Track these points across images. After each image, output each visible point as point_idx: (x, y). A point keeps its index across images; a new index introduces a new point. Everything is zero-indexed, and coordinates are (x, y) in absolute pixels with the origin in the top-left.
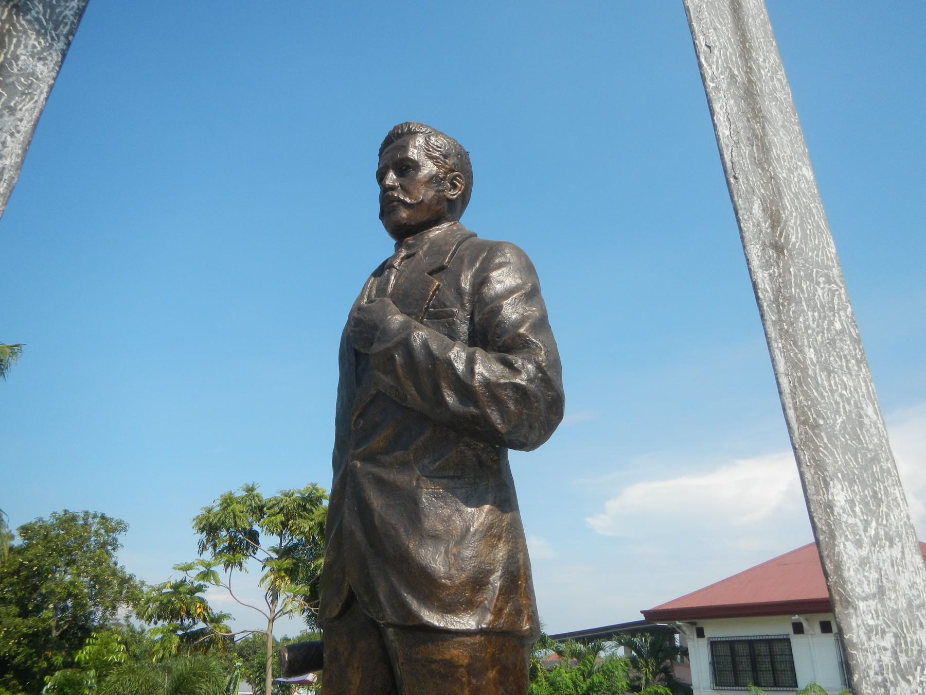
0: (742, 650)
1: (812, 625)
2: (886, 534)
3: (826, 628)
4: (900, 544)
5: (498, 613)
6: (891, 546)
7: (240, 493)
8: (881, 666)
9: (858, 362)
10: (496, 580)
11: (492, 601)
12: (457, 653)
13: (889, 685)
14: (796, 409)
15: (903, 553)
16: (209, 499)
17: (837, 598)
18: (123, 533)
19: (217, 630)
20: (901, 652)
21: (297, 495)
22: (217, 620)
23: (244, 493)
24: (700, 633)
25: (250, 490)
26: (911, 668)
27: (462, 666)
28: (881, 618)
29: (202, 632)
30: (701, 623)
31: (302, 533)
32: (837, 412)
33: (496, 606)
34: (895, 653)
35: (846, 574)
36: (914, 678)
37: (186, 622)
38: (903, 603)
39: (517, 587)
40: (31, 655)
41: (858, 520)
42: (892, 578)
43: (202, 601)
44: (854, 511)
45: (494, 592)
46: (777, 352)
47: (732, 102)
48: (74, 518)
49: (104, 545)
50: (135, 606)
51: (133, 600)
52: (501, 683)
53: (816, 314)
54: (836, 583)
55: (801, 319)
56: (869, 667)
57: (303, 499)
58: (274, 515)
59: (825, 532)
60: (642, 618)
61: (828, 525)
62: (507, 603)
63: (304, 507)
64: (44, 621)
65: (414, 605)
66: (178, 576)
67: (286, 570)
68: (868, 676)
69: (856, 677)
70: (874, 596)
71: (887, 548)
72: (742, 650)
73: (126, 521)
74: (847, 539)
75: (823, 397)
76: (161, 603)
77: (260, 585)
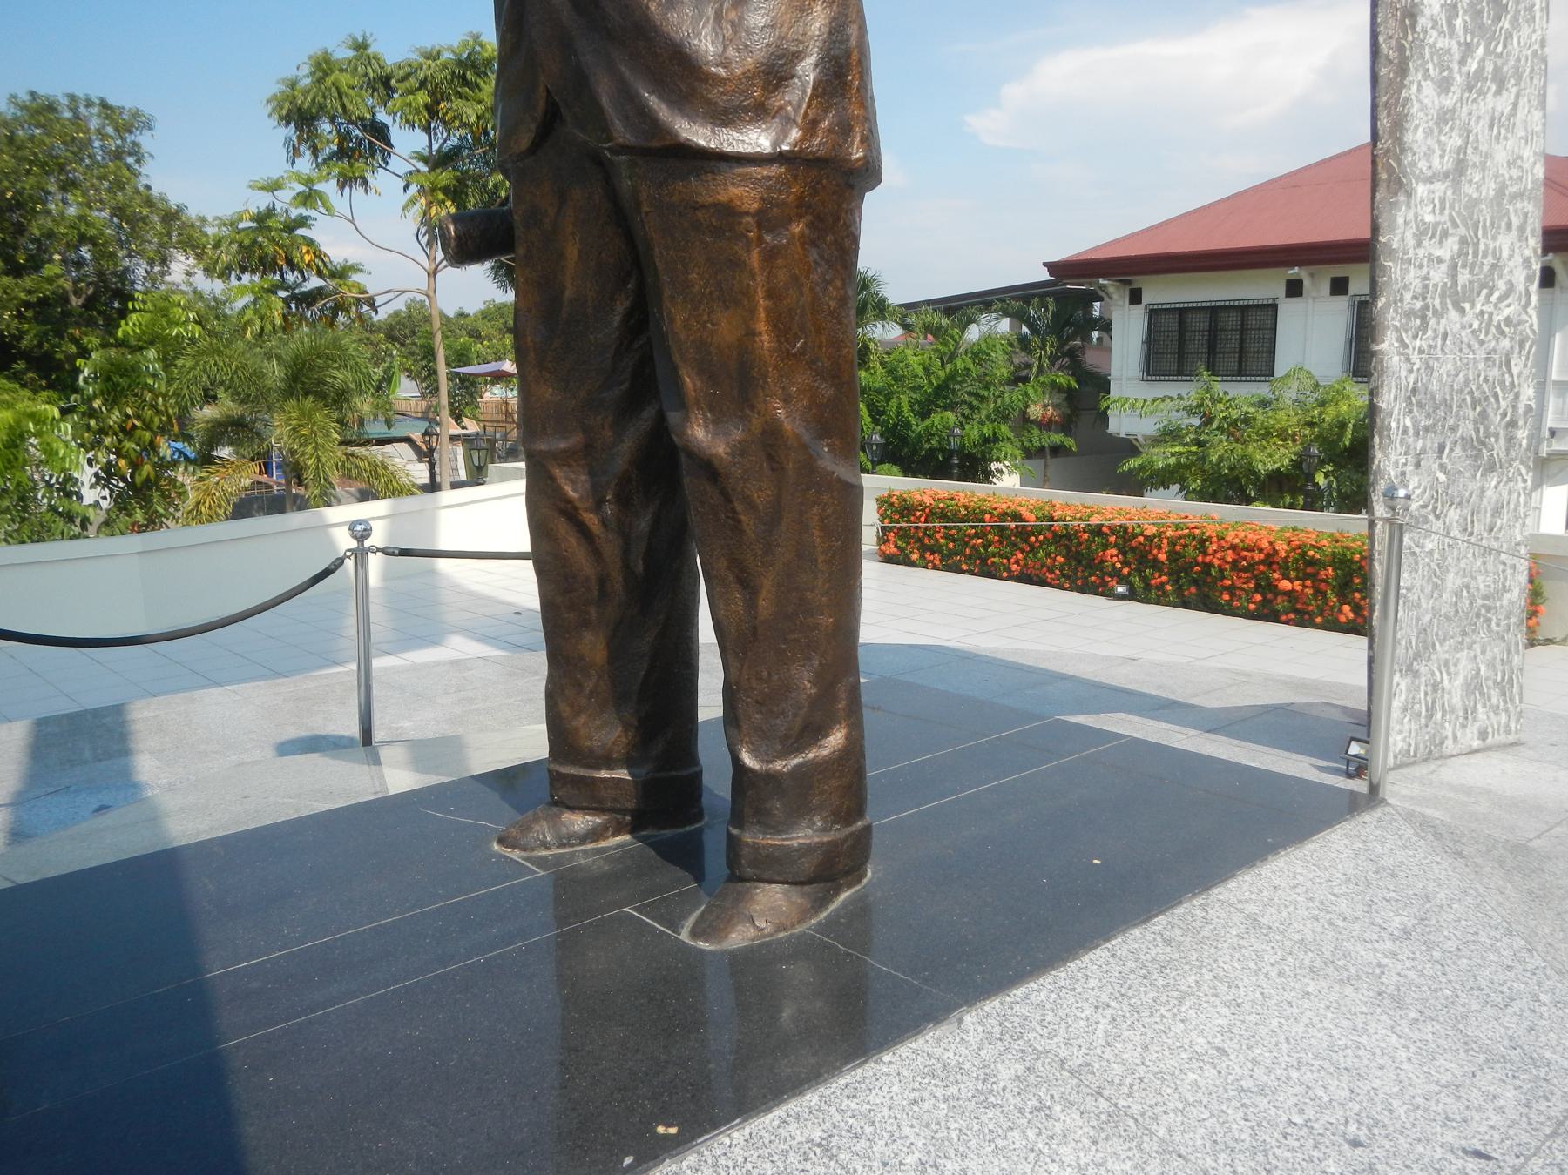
0: (1198, 323)
1: (1317, 283)
2: (1497, 70)
3: (1339, 287)
4: (1514, 90)
5: (810, 127)
6: (1498, 92)
7: (344, 53)
8: (1426, 287)
10: (807, 70)
11: (799, 106)
12: (741, 193)
13: (1430, 314)
15: (1515, 105)
16: (291, 64)
17: (1384, 176)
18: (147, 133)
19: (344, 290)
20: (1464, 266)
21: (447, 56)
22: (341, 273)
23: (351, 54)
24: (1136, 297)
25: (361, 46)
26: (1472, 291)
27: (747, 213)
28: (1447, 212)
29: (319, 293)
30: (1140, 281)
31: (464, 125)
33: (806, 114)
34: (1454, 268)
35: (1408, 137)
36: (1473, 306)
37: (291, 277)
38: (1490, 189)
39: (845, 86)
40: (45, 334)
41: (1454, 43)
42: (1484, 148)
43: (310, 242)
44: (1451, 26)
45: (804, 92)
48: (51, 108)
49: (118, 155)
50: (199, 257)
51: (193, 248)
52: (814, 244)
54: (1388, 151)
56: (1406, 287)
57: (459, 63)
58: (411, 92)
59: (1391, 62)
60: (1044, 275)
61: (1401, 49)
62: (826, 111)
63: (464, 77)
64: (50, 280)
65: (663, 112)
66: (261, 201)
67: (445, 190)
68: (1401, 300)
69: (1381, 302)
70: (1446, 176)
71: (1490, 96)
72: (1198, 323)
73: (147, 109)
74: (1426, 76)
76: (240, 244)
77: (403, 216)
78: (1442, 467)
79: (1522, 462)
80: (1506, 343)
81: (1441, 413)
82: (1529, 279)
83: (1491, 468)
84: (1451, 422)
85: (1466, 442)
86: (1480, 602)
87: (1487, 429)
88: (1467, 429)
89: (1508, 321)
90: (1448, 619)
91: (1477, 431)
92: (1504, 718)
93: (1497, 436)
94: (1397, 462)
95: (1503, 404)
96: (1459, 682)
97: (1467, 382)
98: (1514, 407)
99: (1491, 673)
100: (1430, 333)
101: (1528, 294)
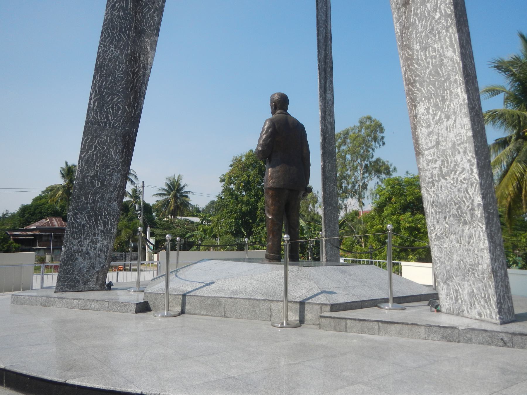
4: (454, 118)
6: (448, 120)
8: (432, 176)
13: (435, 182)
20: (444, 167)
26: (448, 173)
34: (441, 169)
35: (420, 142)
36: (450, 177)
38: (450, 145)
41: (430, 116)
42: (445, 136)
53: (423, 22)
55: (414, 32)
70: (434, 147)
74: (422, 126)
75: (420, 65)
78: (447, 223)
79: (479, 222)
80: (465, 185)
81: (444, 208)
82: (472, 165)
83: (465, 223)
84: (448, 210)
85: (454, 216)
86: (469, 266)
87: (461, 211)
88: (454, 211)
89: (464, 179)
90: (457, 269)
91: (458, 212)
92: (488, 312)
93: (466, 214)
94: (431, 222)
95: (467, 204)
96: (466, 292)
97: (452, 198)
98: (472, 204)
99: (478, 292)
100: (436, 187)
101: (472, 170)
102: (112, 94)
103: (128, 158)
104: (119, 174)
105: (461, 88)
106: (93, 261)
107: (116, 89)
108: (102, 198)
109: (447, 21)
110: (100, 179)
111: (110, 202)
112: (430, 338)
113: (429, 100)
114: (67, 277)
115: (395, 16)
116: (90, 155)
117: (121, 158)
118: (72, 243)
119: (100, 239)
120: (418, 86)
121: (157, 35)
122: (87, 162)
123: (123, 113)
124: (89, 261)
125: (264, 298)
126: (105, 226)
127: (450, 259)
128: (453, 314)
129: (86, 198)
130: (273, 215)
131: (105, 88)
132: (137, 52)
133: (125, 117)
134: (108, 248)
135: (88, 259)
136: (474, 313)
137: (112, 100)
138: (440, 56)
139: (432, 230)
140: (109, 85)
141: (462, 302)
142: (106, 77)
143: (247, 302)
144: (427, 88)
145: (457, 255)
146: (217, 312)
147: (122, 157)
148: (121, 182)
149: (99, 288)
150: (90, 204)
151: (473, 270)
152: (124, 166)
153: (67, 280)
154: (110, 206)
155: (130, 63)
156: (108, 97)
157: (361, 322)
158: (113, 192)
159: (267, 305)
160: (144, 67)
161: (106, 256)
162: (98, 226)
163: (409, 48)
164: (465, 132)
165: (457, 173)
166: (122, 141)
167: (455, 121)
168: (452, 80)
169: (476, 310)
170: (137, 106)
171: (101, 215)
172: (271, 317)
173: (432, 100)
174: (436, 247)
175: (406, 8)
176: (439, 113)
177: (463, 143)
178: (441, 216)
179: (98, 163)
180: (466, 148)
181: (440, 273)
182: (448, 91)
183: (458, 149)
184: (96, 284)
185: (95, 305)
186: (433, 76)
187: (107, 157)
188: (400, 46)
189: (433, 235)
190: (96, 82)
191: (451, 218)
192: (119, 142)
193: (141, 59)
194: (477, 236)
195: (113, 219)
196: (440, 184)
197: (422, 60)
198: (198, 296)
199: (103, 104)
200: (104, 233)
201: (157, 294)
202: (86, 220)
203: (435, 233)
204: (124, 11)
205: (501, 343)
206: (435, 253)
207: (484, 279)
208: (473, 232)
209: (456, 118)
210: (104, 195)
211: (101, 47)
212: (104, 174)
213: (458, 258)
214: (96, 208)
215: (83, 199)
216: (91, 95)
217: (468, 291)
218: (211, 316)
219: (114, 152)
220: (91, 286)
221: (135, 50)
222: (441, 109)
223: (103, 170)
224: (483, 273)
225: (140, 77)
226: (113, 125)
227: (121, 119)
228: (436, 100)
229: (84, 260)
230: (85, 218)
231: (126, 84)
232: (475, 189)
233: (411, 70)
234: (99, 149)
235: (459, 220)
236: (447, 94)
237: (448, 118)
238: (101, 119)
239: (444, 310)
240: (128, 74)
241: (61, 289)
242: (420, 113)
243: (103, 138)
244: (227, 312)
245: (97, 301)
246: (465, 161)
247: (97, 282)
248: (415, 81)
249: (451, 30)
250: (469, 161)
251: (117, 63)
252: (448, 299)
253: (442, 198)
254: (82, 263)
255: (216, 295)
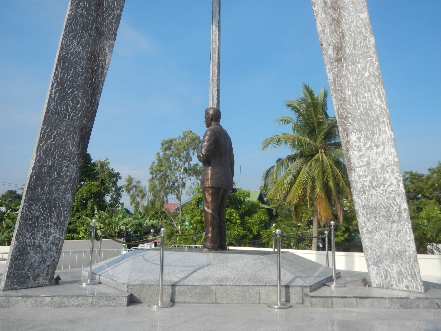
4: (382, 147)
9: (376, 86)
14: (338, 115)
20: (374, 181)
28: (366, 172)
32: (359, 109)
34: (371, 182)
35: (352, 161)
36: (379, 188)
41: (361, 144)
46: (333, 99)
47: (323, 15)
53: (355, 76)
55: (346, 82)
61: (347, 148)
69: (352, 190)
70: (365, 166)
74: (354, 150)
75: (351, 106)
78: (377, 221)
79: (406, 221)
81: (374, 210)
83: (394, 222)
84: (378, 212)
85: (383, 216)
86: (397, 253)
89: (392, 191)
90: (387, 255)
91: (387, 214)
92: (415, 285)
93: (394, 215)
94: (362, 220)
95: (395, 208)
96: (395, 271)
99: (406, 271)
100: (367, 194)
102: (73, 87)
103: (83, 151)
104: (75, 166)
105: (388, 128)
106: (44, 255)
107: (76, 83)
108: (57, 189)
109: (375, 80)
110: (57, 170)
111: (64, 193)
112: (393, 307)
113: (360, 132)
114: (17, 273)
115: (328, 67)
116: (49, 145)
117: (77, 151)
118: (25, 236)
119: (53, 231)
120: (350, 121)
121: (114, 39)
122: (45, 152)
123: (82, 107)
124: (41, 255)
125: (253, 284)
126: (58, 218)
127: (381, 247)
128: (383, 288)
129: (42, 189)
130: (212, 210)
131: (66, 81)
132: (97, 52)
133: (83, 111)
134: (59, 241)
135: (39, 253)
136: (402, 286)
137: (72, 92)
138: (370, 102)
139: (364, 226)
140: (70, 78)
141: (391, 278)
142: (68, 70)
143: (237, 289)
144: (358, 123)
145: (387, 245)
146: (208, 299)
147: (79, 148)
148: (76, 174)
149: (48, 283)
150: (46, 195)
151: (401, 255)
152: (79, 159)
153: (17, 276)
154: (65, 198)
155: (90, 60)
156: (69, 89)
157: (344, 299)
158: (68, 184)
159: (256, 289)
160: (102, 66)
161: (57, 249)
162: (51, 218)
163: (341, 92)
164: (392, 158)
165: (386, 186)
166: (80, 134)
167: (384, 150)
168: (381, 120)
169: (404, 284)
170: (94, 102)
171: (55, 207)
172: (260, 300)
173: (363, 133)
174: (367, 238)
175: (338, 64)
176: (370, 142)
177: (391, 165)
178: (371, 216)
179: (56, 154)
180: (393, 169)
181: (371, 258)
182: (377, 128)
183: (386, 169)
184: (46, 279)
185: (75, 301)
186: (364, 115)
187: (64, 148)
188: (332, 89)
189: (364, 230)
190: (58, 73)
191: (381, 218)
192: (76, 135)
193: (100, 58)
194: (404, 231)
195: (66, 211)
196: (370, 193)
197: (353, 103)
198: (188, 285)
199: (64, 96)
200: (57, 225)
201: (143, 286)
202: (41, 212)
203: (366, 229)
204: (87, 11)
205: (436, 307)
206: (366, 242)
207: (410, 261)
208: (401, 228)
209: (384, 148)
210: (59, 186)
211: (65, 40)
212: (61, 165)
213: (388, 247)
214: (51, 200)
215: (39, 190)
216: (53, 85)
217: (397, 271)
218: (202, 303)
219: (71, 144)
220: (40, 282)
221: (95, 49)
222: (372, 140)
223: (60, 161)
224: (410, 258)
225: (98, 75)
226: (72, 117)
227: (79, 112)
228: (366, 133)
229: (36, 254)
230: (40, 209)
231: (86, 80)
232: (402, 198)
233: (343, 108)
234: (58, 140)
235: (388, 220)
236: (376, 129)
237: (377, 146)
238: (61, 110)
239: (374, 285)
240: (88, 71)
241: (10, 286)
242: (352, 140)
243: (61, 129)
244: (218, 299)
245: (78, 296)
246: (392, 178)
247: (46, 276)
248: (347, 117)
249: (379, 87)
250: (396, 178)
251: (78, 59)
252: (378, 277)
253: (372, 203)
254: (34, 257)
255: (204, 283)
